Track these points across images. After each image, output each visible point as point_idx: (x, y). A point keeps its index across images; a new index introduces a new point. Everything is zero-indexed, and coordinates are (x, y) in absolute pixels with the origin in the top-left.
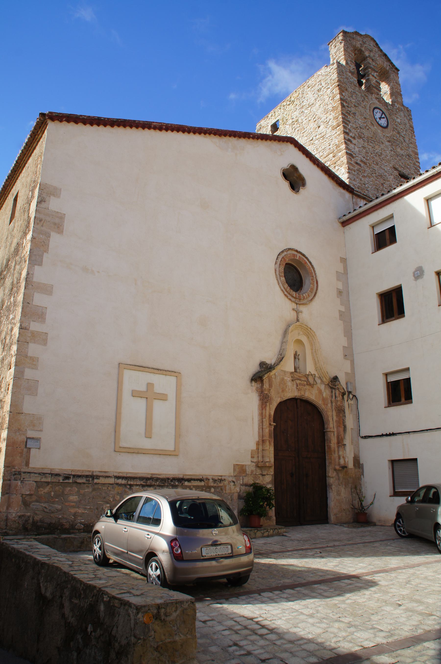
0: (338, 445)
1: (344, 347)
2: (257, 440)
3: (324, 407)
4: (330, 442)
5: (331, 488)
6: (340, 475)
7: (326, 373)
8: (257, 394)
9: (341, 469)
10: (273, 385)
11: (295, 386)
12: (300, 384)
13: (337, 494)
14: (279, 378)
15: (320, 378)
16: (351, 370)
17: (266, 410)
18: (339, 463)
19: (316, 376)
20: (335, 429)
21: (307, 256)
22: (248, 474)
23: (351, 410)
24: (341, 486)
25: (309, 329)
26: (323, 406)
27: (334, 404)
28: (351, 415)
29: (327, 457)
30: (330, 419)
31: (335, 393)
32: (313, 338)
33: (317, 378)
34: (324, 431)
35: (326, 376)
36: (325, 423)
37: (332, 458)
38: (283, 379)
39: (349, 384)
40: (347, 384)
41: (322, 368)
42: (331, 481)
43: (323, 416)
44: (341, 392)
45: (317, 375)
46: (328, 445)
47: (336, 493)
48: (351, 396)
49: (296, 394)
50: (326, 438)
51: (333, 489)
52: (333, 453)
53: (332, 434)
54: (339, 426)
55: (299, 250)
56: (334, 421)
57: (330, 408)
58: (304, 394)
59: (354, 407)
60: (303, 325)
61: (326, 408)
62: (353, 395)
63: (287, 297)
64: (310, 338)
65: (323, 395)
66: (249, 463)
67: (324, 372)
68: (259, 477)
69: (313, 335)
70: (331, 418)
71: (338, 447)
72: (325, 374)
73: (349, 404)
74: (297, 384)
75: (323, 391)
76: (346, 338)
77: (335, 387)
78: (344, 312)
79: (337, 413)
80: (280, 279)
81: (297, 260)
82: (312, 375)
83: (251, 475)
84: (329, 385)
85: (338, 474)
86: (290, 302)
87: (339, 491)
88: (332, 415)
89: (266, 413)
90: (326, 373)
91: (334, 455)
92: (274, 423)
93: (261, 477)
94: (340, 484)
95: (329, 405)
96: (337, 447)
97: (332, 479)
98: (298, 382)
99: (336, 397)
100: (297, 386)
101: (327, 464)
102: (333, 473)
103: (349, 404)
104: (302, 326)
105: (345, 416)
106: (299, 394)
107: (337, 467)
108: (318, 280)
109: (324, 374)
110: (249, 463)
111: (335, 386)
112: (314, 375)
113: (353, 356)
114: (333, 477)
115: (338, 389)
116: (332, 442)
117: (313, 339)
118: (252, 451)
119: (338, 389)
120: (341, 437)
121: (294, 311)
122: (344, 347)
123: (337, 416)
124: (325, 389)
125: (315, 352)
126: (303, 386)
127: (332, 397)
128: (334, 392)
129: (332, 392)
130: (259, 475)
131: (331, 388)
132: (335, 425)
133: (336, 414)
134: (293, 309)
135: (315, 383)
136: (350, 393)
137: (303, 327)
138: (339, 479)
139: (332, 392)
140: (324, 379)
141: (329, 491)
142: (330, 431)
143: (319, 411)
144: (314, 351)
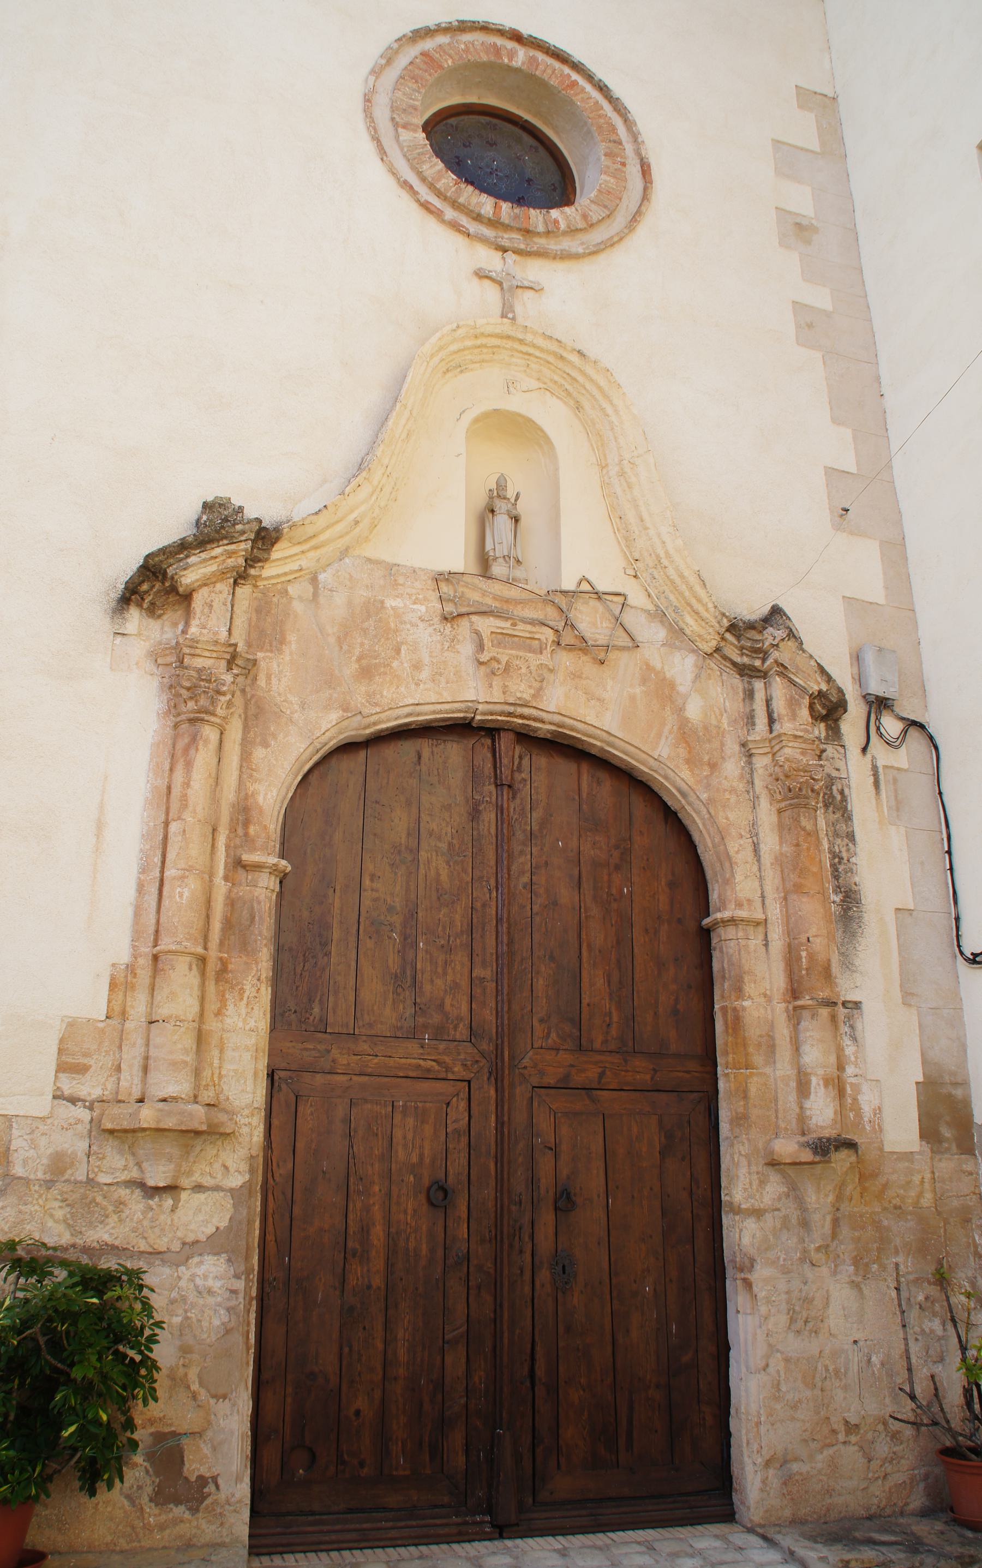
0: (795, 1008)
1: (830, 472)
2: (124, 957)
3: (691, 781)
4: (739, 990)
5: (748, 1284)
6: (812, 1198)
7: (693, 580)
8: (155, 683)
9: (807, 1156)
10: (292, 637)
11: (467, 649)
12: (502, 638)
13: (792, 1320)
14: (340, 599)
15: (659, 615)
16: (886, 588)
17: (189, 765)
18: (802, 1118)
19: (630, 601)
20: (775, 911)
21: (577, 54)
22: (27, 1181)
23: (898, 805)
24: (824, 1271)
25: (574, 358)
26: (685, 774)
27: (761, 762)
28: (896, 837)
29: (721, 1085)
30: (739, 849)
31: (768, 702)
32: (605, 405)
33: (643, 618)
34: (706, 922)
35: (699, 600)
36: (709, 874)
37: (753, 1090)
38: (373, 609)
39: (869, 658)
40: (857, 658)
41: (667, 553)
42: (746, 1240)
43: (696, 837)
44: (803, 690)
45: (637, 598)
46: (724, 1009)
47: (783, 1319)
48: (891, 726)
49: (469, 693)
50: (716, 966)
51: (761, 1291)
52: (758, 1059)
53: (755, 942)
54: (798, 889)
55: (525, 31)
56: (767, 859)
57: (741, 786)
58: (538, 694)
59: (920, 790)
60: (529, 338)
61: (708, 787)
62: (902, 719)
63: (437, 214)
64: (586, 404)
65: (681, 710)
66: (41, 1105)
67: (682, 576)
68: (120, 1204)
69: (599, 388)
70: (747, 843)
71: (795, 1015)
72: (691, 589)
73: (875, 769)
74: (477, 633)
75: (682, 689)
76: (847, 433)
77: (764, 660)
78: (828, 315)
79: (780, 811)
80: (397, 137)
81: (517, 70)
82: (598, 596)
83: (49, 1184)
84: (725, 658)
85: (794, 1190)
86: (460, 240)
87: (807, 1301)
88: (754, 825)
89: (187, 785)
90: (693, 580)
91: (768, 1070)
92: (282, 856)
93: (136, 1203)
94: (815, 1256)
95: (732, 768)
96: (789, 1018)
97: (750, 1225)
98: (486, 625)
99: (771, 721)
100: (481, 647)
101: (725, 1128)
102: (762, 1183)
103: (875, 769)
104: (521, 341)
105: (851, 837)
106: (497, 696)
107: (787, 1147)
108: (653, 161)
109: (683, 588)
110: (41, 1105)
111: (765, 655)
112: (620, 599)
113: (899, 523)
114: (758, 1213)
115: (783, 670)
116: (749, 988)
117: (603, 410)
118: (72, 1025)
119: (780, 674)
120: (811, 957)
121: (487, 283)
122: (830, 472)
123: (781, 827)
124: (697, 677)
125: (622, 474)
126: (531, 650)
127: (750, 720)
128: (760, 696)
129: (750, 695)
130: (123, 1192)
131: (745, 671)
132: (769, 889)
133: (774, 818)
134: (481, 275)
135: (623, 640)
136: (880, 704)
137: (534, 346)
138: (805, 1224)
139: (750, 695)
140: (689, 620)
141: (737, 1299)
142: (733, 921)
143: (665, 804)
144: (614, 470)
